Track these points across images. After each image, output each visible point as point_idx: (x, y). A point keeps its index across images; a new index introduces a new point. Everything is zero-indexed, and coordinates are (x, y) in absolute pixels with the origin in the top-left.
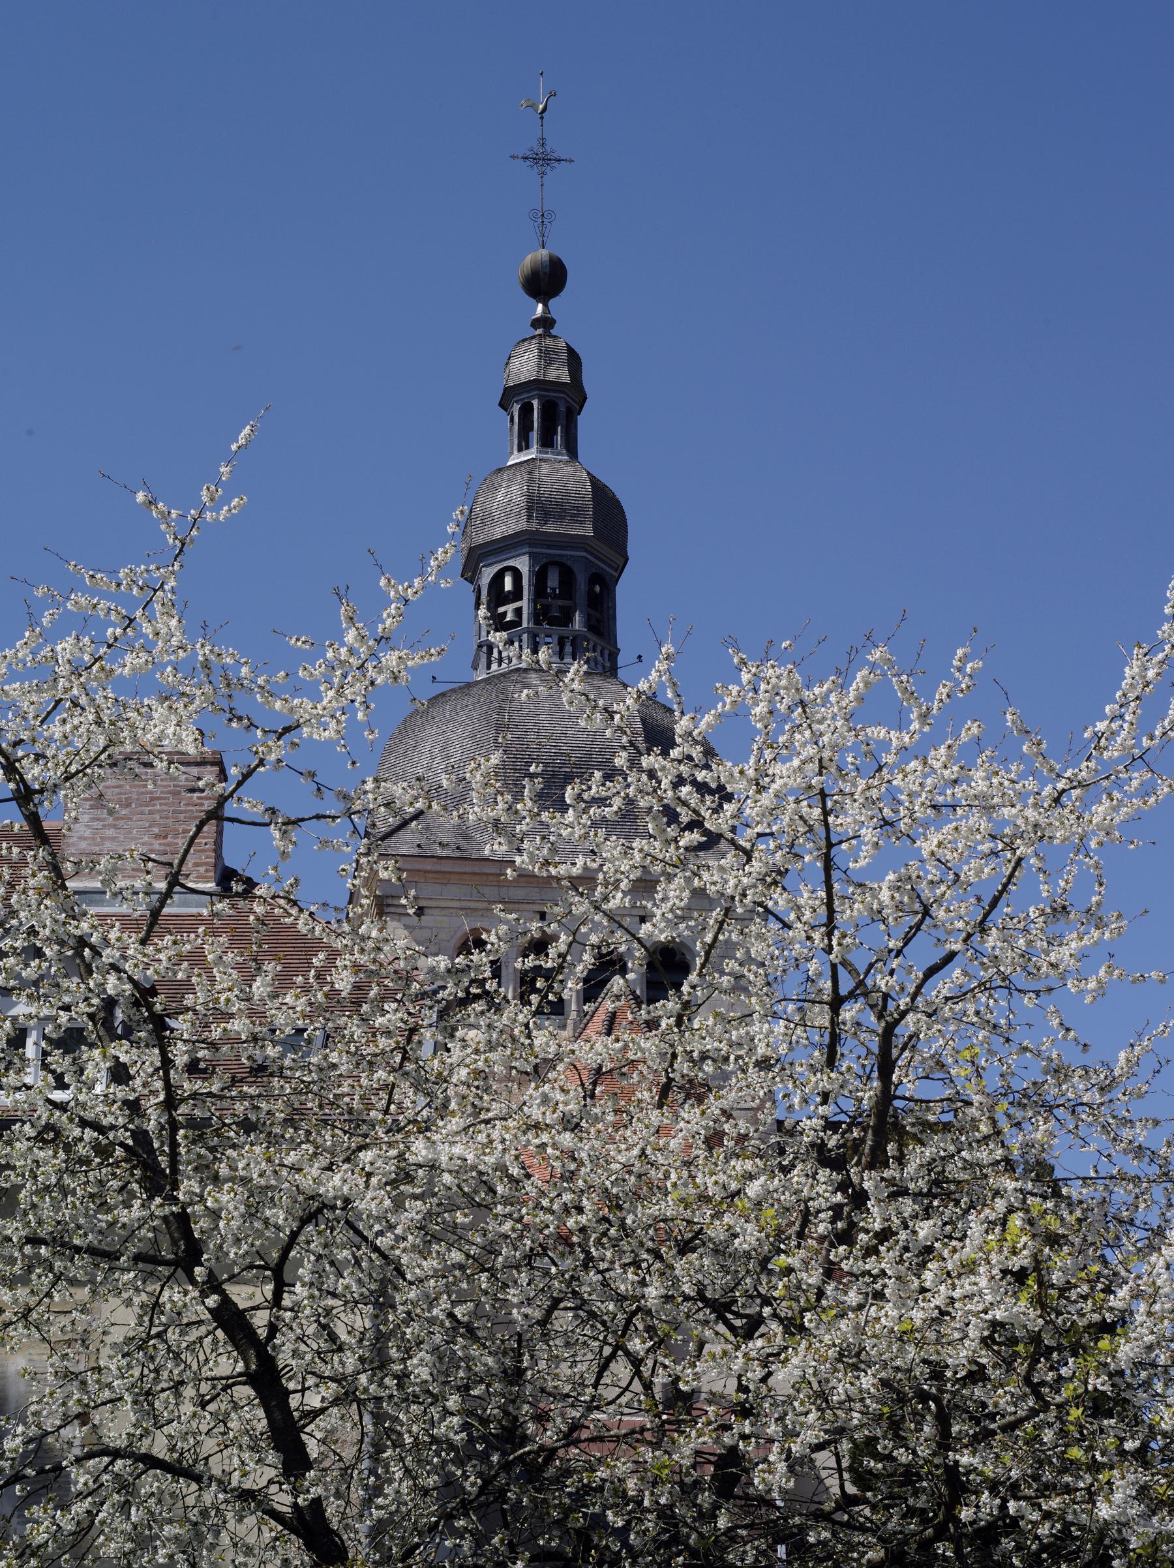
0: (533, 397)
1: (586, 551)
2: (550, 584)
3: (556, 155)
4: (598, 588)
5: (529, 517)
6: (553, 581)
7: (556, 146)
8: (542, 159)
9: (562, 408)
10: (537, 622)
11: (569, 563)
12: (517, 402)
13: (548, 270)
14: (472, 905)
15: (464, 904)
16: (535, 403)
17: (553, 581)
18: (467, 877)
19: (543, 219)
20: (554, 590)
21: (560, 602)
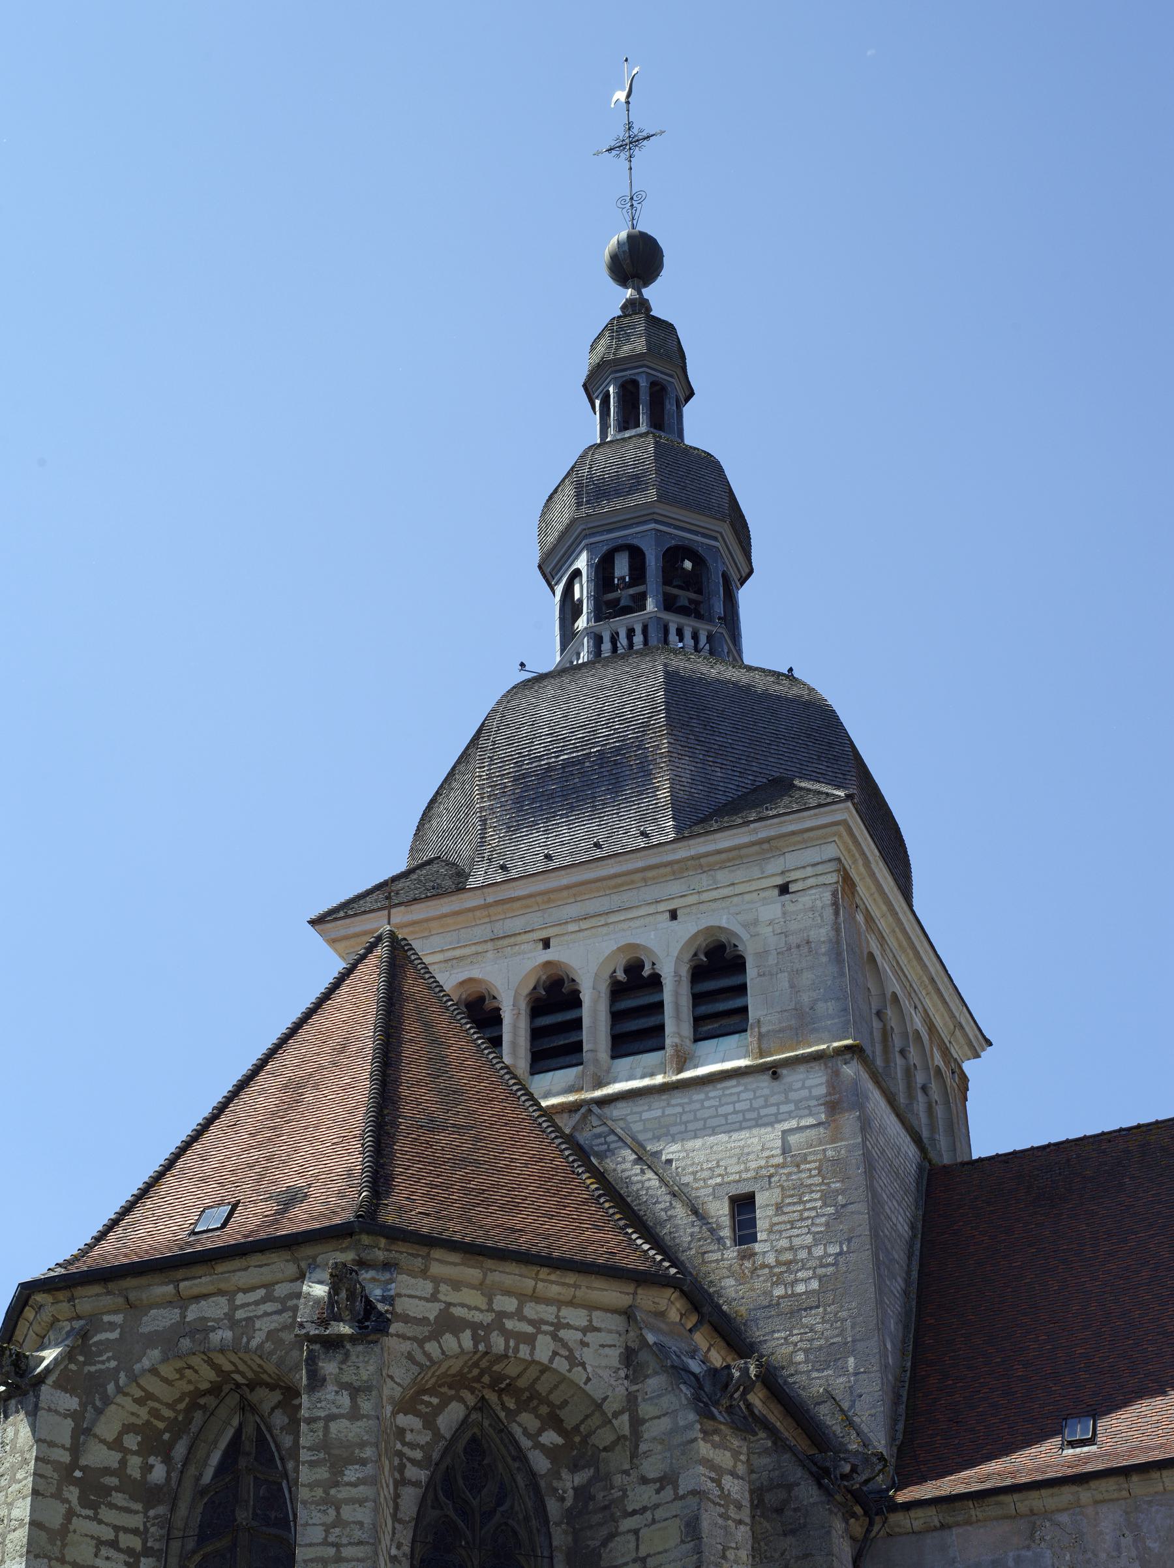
0: (608, 385)
1: (656, 522)
2: (617, 573)
3: (645, 134)
4: (688, 565)
5: (579, 504)
6: (622, 568)
7: (642, 125)
8: (630, 143)
9: (643, 383)
10: (598, 618)
11: (635, 542)
12: (597, 398)
13: (626, 248)
14: (457, 953)
15: (449, 955)
16: (611, 389)
17: (622, 568)
18: (449, 920)
19: (633, 201)
20: (622, 578)
21: (632, 591)
